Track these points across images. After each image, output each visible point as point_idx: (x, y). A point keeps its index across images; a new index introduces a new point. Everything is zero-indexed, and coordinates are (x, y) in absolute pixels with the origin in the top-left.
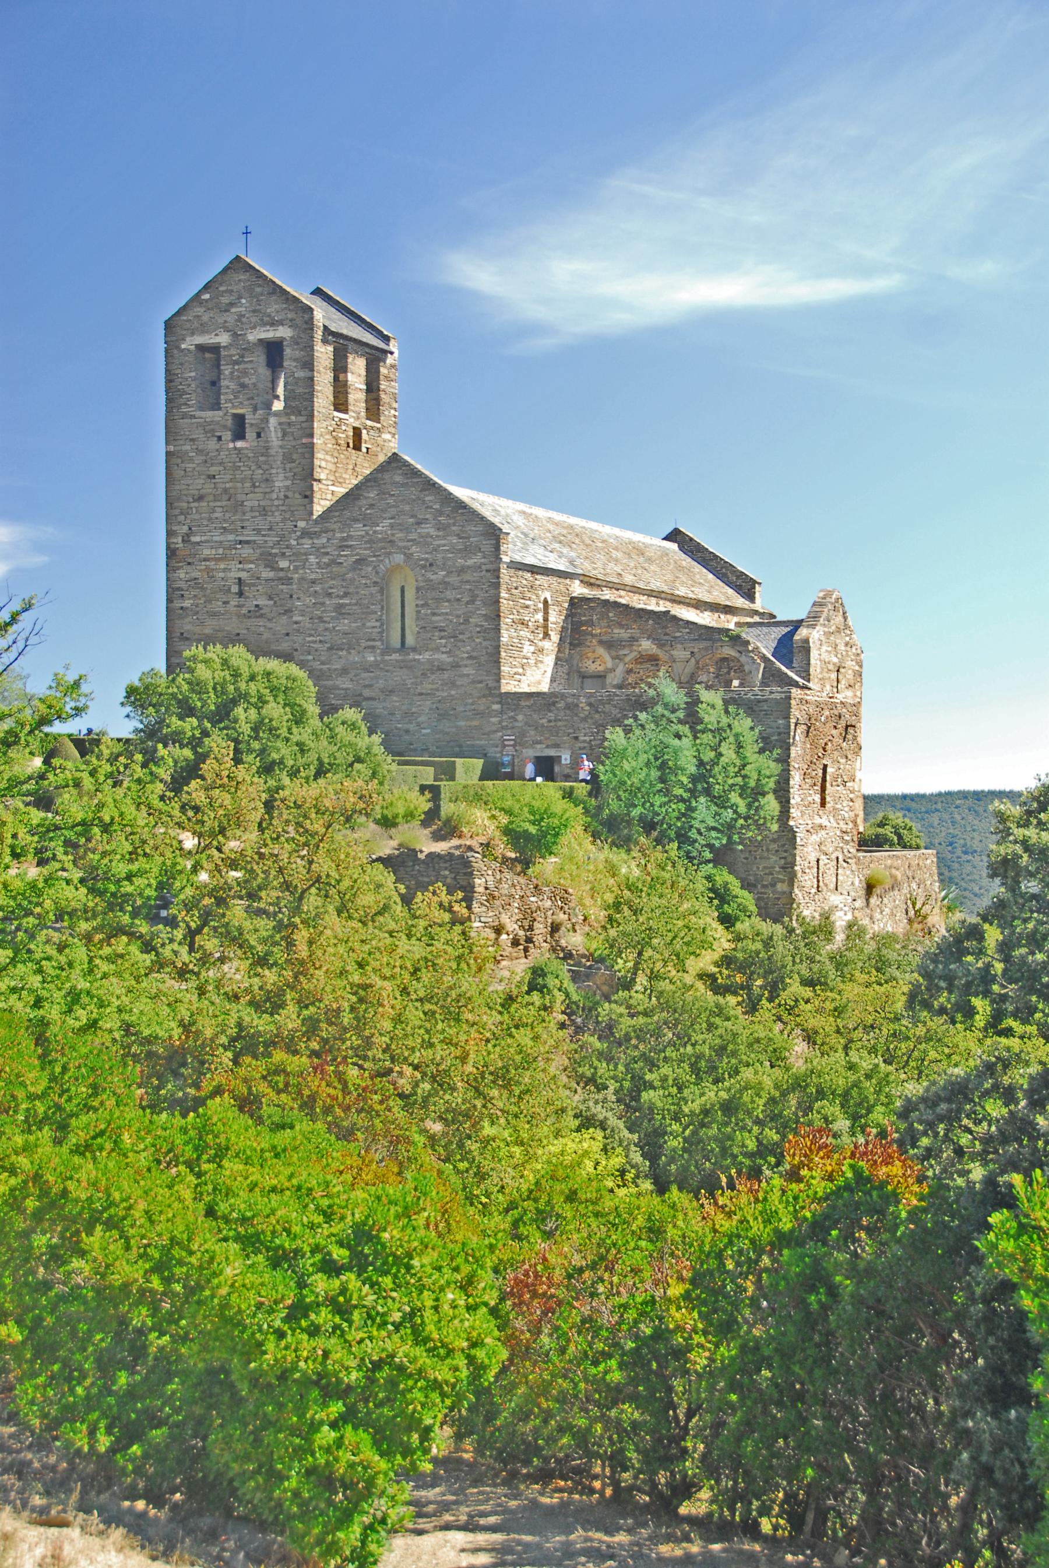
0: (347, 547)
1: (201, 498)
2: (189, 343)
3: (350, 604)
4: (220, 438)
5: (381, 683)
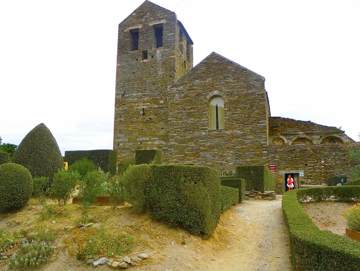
0: (193, 90)
1: (129, 80)
2: (128, 29)
3: (194, 112)
4: (137, 59)
5: (208, 144)
